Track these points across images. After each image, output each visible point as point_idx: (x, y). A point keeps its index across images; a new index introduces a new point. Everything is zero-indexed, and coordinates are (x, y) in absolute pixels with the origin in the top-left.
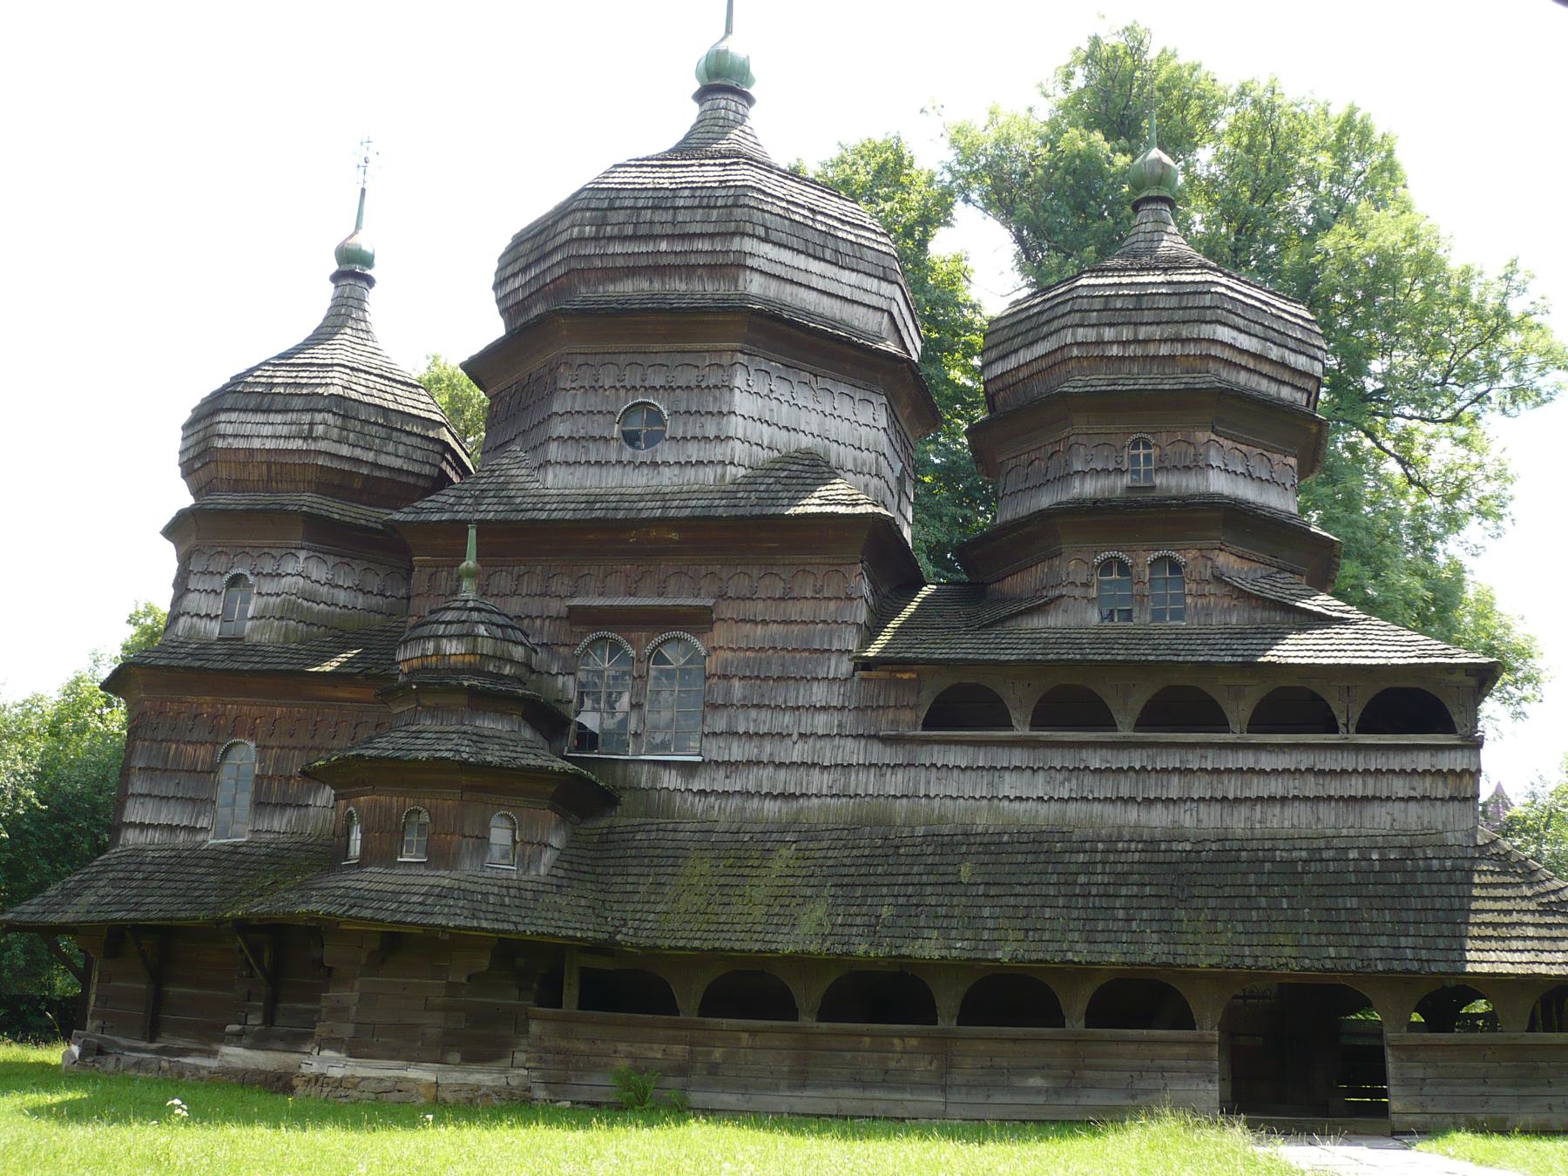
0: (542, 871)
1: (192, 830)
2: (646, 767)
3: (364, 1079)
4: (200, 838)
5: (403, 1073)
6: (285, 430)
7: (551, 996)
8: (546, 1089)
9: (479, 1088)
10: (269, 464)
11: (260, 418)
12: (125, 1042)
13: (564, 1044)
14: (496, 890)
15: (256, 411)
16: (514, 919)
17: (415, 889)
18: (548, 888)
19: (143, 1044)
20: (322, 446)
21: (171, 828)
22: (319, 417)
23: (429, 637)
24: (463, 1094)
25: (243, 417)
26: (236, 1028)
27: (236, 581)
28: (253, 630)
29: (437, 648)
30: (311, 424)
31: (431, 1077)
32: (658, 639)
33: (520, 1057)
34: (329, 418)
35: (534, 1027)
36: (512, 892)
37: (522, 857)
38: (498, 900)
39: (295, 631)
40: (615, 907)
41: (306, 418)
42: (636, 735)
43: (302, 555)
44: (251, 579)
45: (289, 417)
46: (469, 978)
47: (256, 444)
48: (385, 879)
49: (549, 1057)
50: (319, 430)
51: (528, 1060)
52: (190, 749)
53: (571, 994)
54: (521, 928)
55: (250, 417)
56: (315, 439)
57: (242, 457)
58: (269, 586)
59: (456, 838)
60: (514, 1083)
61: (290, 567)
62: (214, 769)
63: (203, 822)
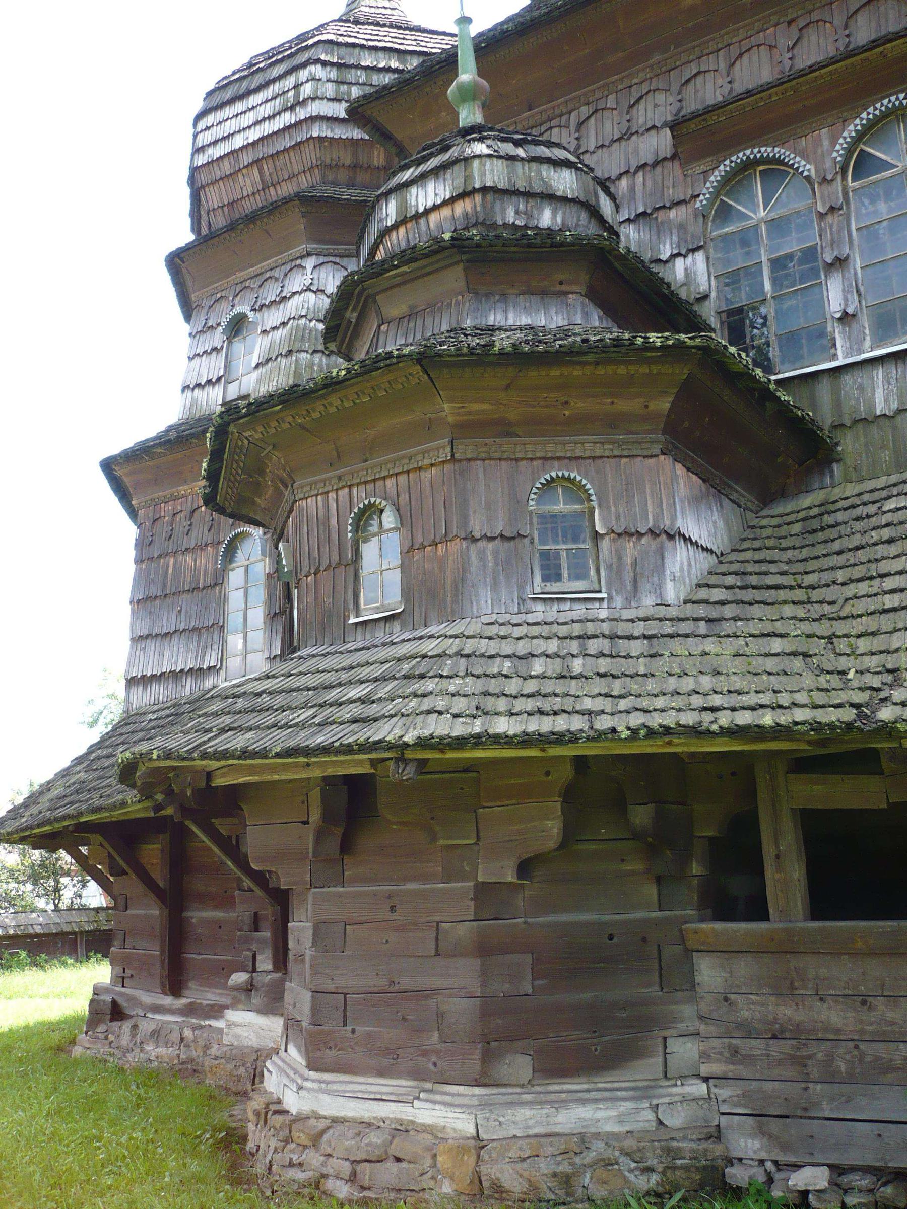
0: (672, 593)
1: (198, 673)
2: (879, 374)
3: (335, 1121)
4: (208, 683)
5: (404, 1112)
6: (268, 109)
7: (736, 894)
8: (762, 1132)
9: (583, 1140)
10: (257, 162)
11: (239, 107)
12: (147, 998)
13: (787, 1012)
14: (552, 646)
15: (232, 101)
16: (587, 704)
17: (365, 672)
18: (685, 627)
19: (168, 1001)
20: (315, 108)
21: (176, 676)
22: (304, 74)
23: (387, 195)
24: (545, 1166)
25: (220, 115)
26: (239, 978)
27: (237, 327)
28: (259, 381)
29: (403, 206)
30: (297, 87)
31: (461, 1124)
32: (851, 130)
33: (684, 1051)
34: (317, 70)
35: (709, 973)
36: (593, 646)
37: (616, 570)
38: (555, 666)
39: (311, 365)
40: (863, 645)
41: (290, 82)
42: (846, 318)
43: (310, 263)
44: (251, 315)
45: (269, 92)
46: (524, 868)
47: (238, 141)
48: (324, 664)
49: (756, 1047)
50: (307, 90)
51: (705, 1056)
52: (189, 558)
53: (786, 877)
54: (603, 723)
55: (229, 111)
56: (303, 103)
57: (227, 167)
58: (273, 318)
59: (455, 546)
60: (675, 1120)
61: (297, 282)
62: (219, 581)
63: (211, 660)
